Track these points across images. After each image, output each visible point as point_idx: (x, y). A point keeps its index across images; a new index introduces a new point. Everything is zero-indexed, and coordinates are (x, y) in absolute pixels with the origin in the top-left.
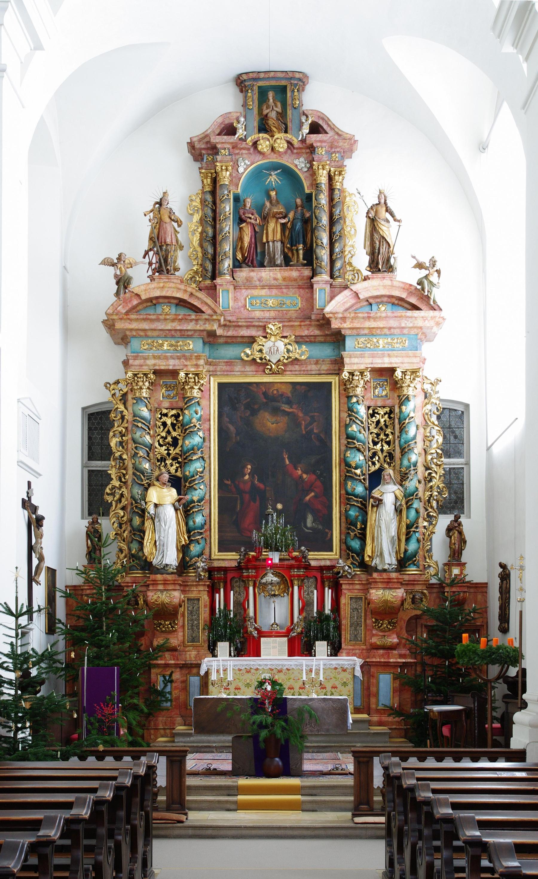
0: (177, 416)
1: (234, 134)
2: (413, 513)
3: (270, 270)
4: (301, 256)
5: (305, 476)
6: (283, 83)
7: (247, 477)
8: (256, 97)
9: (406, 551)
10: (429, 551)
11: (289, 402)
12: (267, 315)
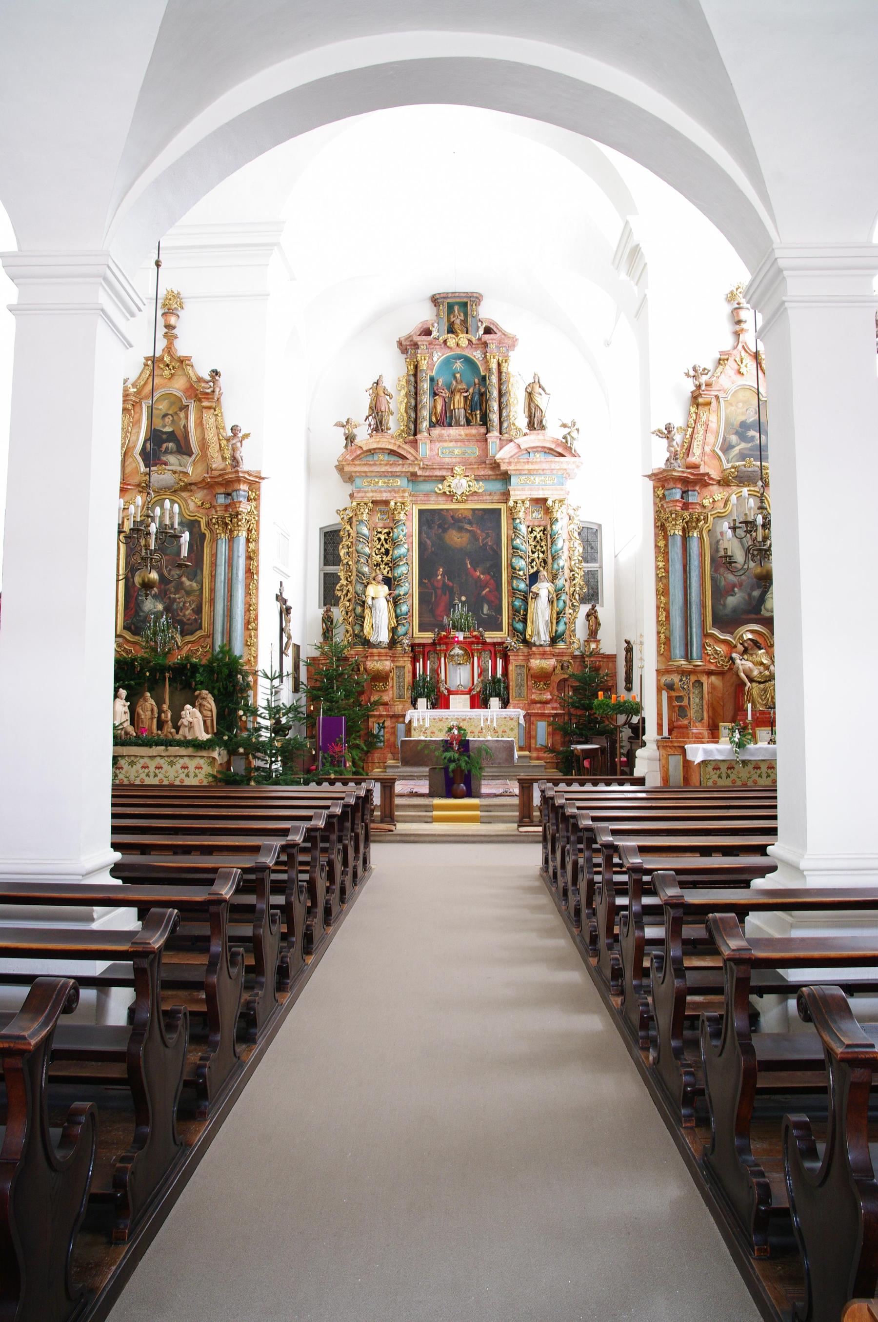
0: (388, 534)
1: (430, 334)
2: (561, 603)
4: (478, 419)
5: (482, 576)
6: (465, 300)
7: (439, 577)
8: (446, 309)
9: (556, 631)
10: (574, 631)
11: (470, 523)
12: (454, 460)
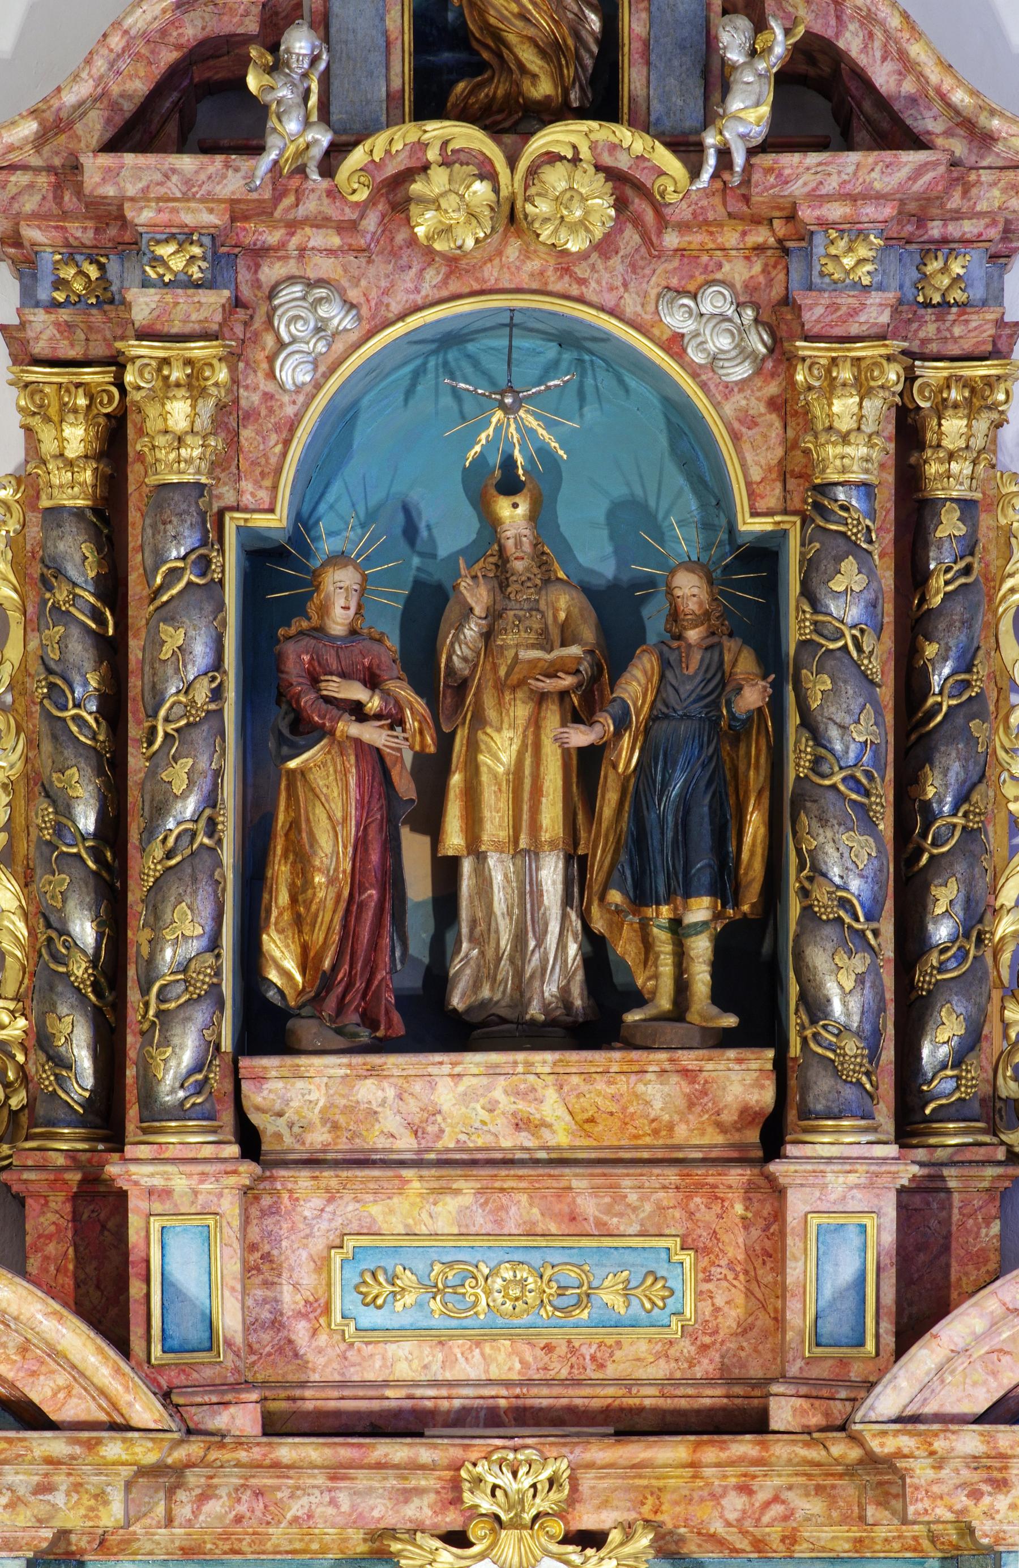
3: (493, 1072)
4: (701, 978)
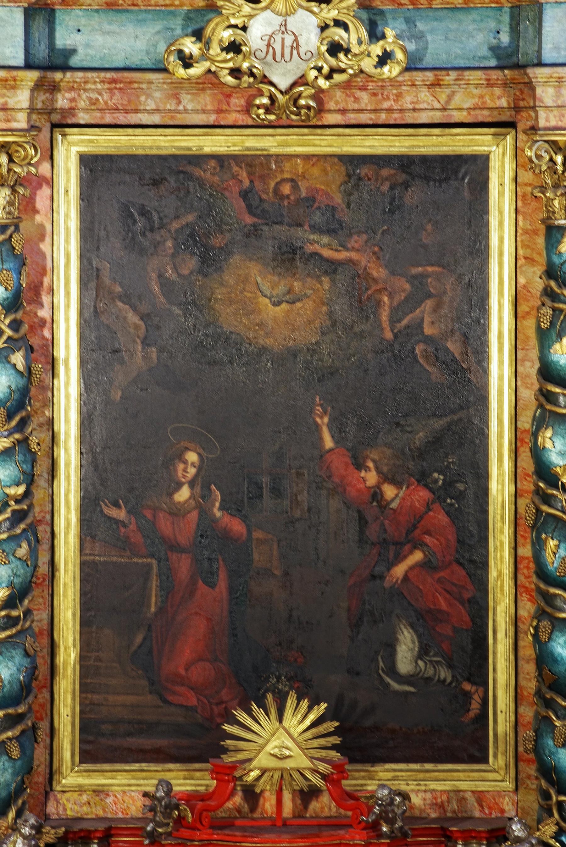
5: (389, 491)
11: (333, 228)
